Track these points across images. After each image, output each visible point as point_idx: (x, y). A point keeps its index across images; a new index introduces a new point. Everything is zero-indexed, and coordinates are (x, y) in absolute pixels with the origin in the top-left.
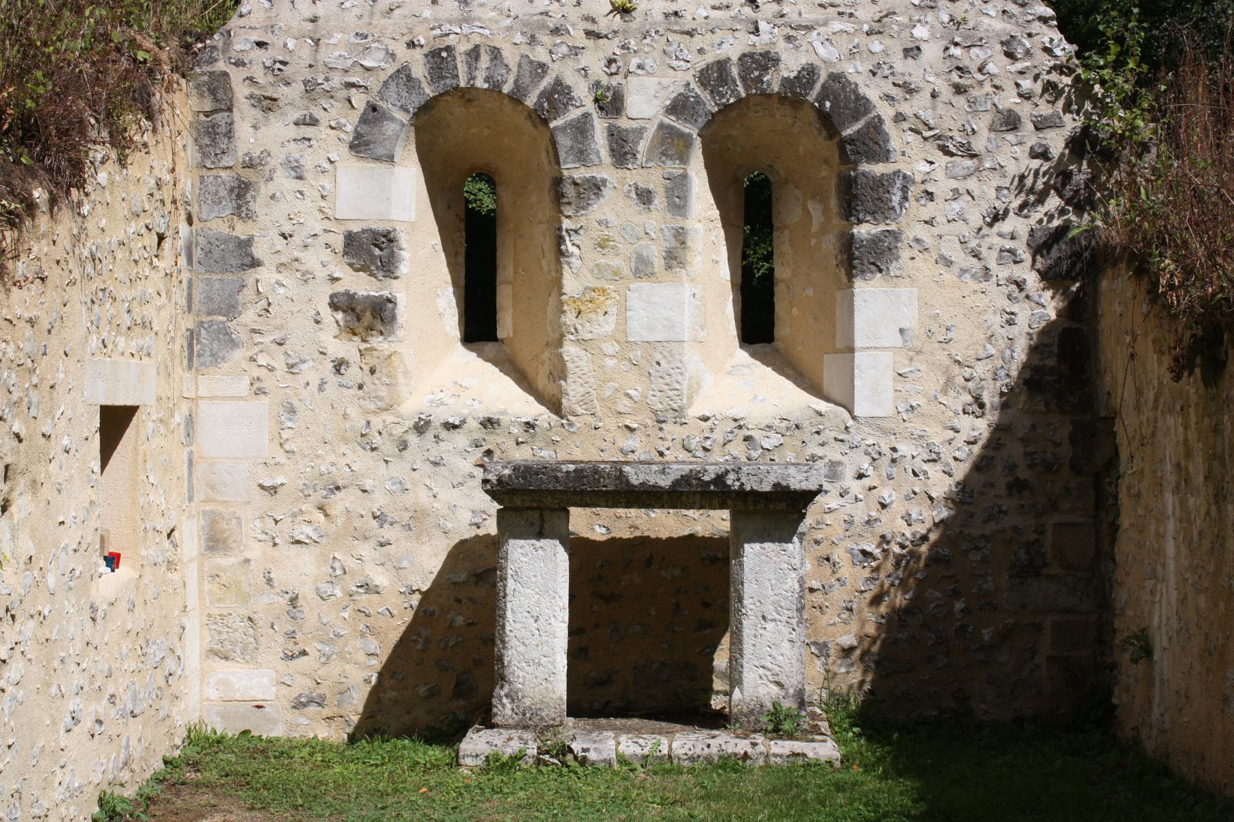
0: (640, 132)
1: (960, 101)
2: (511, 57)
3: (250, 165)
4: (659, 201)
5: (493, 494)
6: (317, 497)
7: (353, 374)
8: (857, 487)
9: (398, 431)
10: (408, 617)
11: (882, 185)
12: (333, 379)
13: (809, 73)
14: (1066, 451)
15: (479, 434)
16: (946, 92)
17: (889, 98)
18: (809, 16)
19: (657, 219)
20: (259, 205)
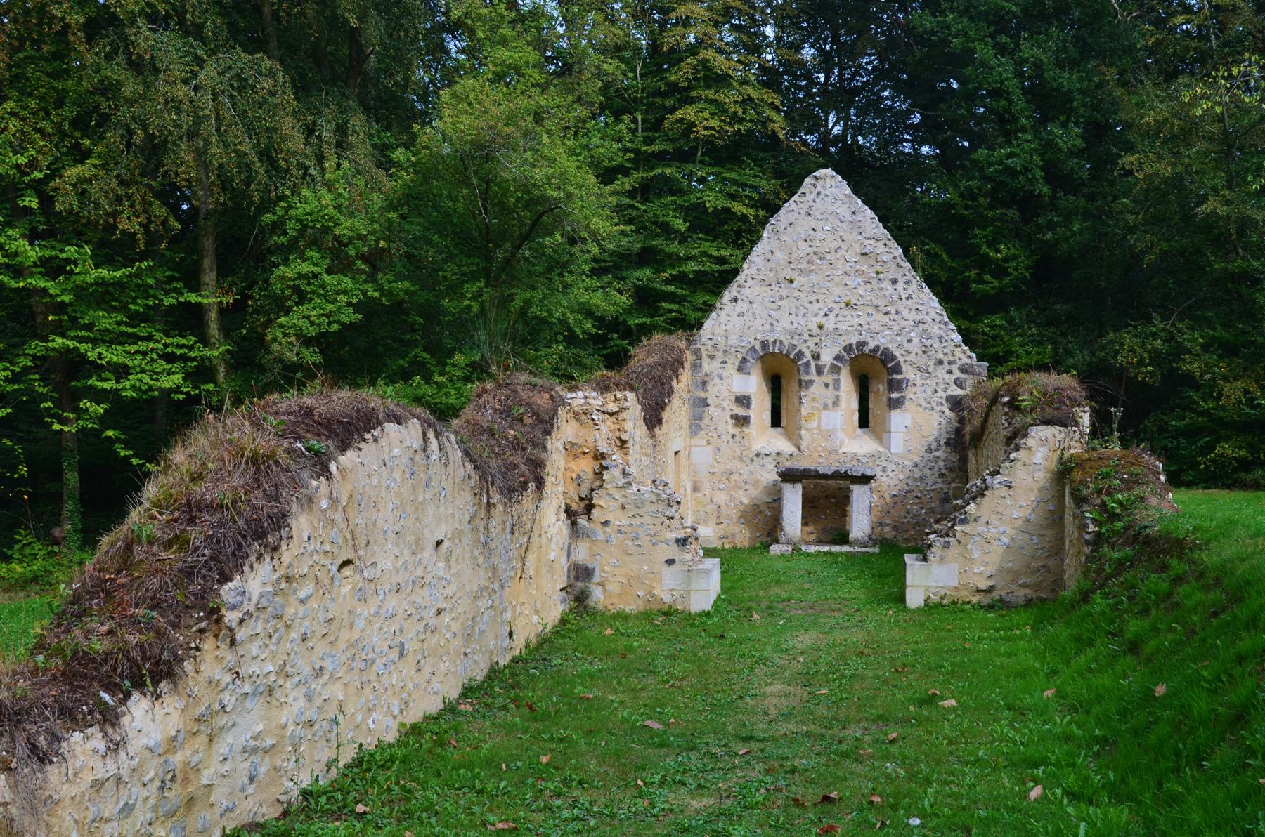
0: (825, 365)
1: (925, 356)
2: (786, 343)
4: (831, 387)
5: (780, 476)
7: (737, 439)
8: (892, 475)
11: (900, 381)
13: (877, 348)
16: (920, 353)
19: (830, 392)
20: (709, 388)
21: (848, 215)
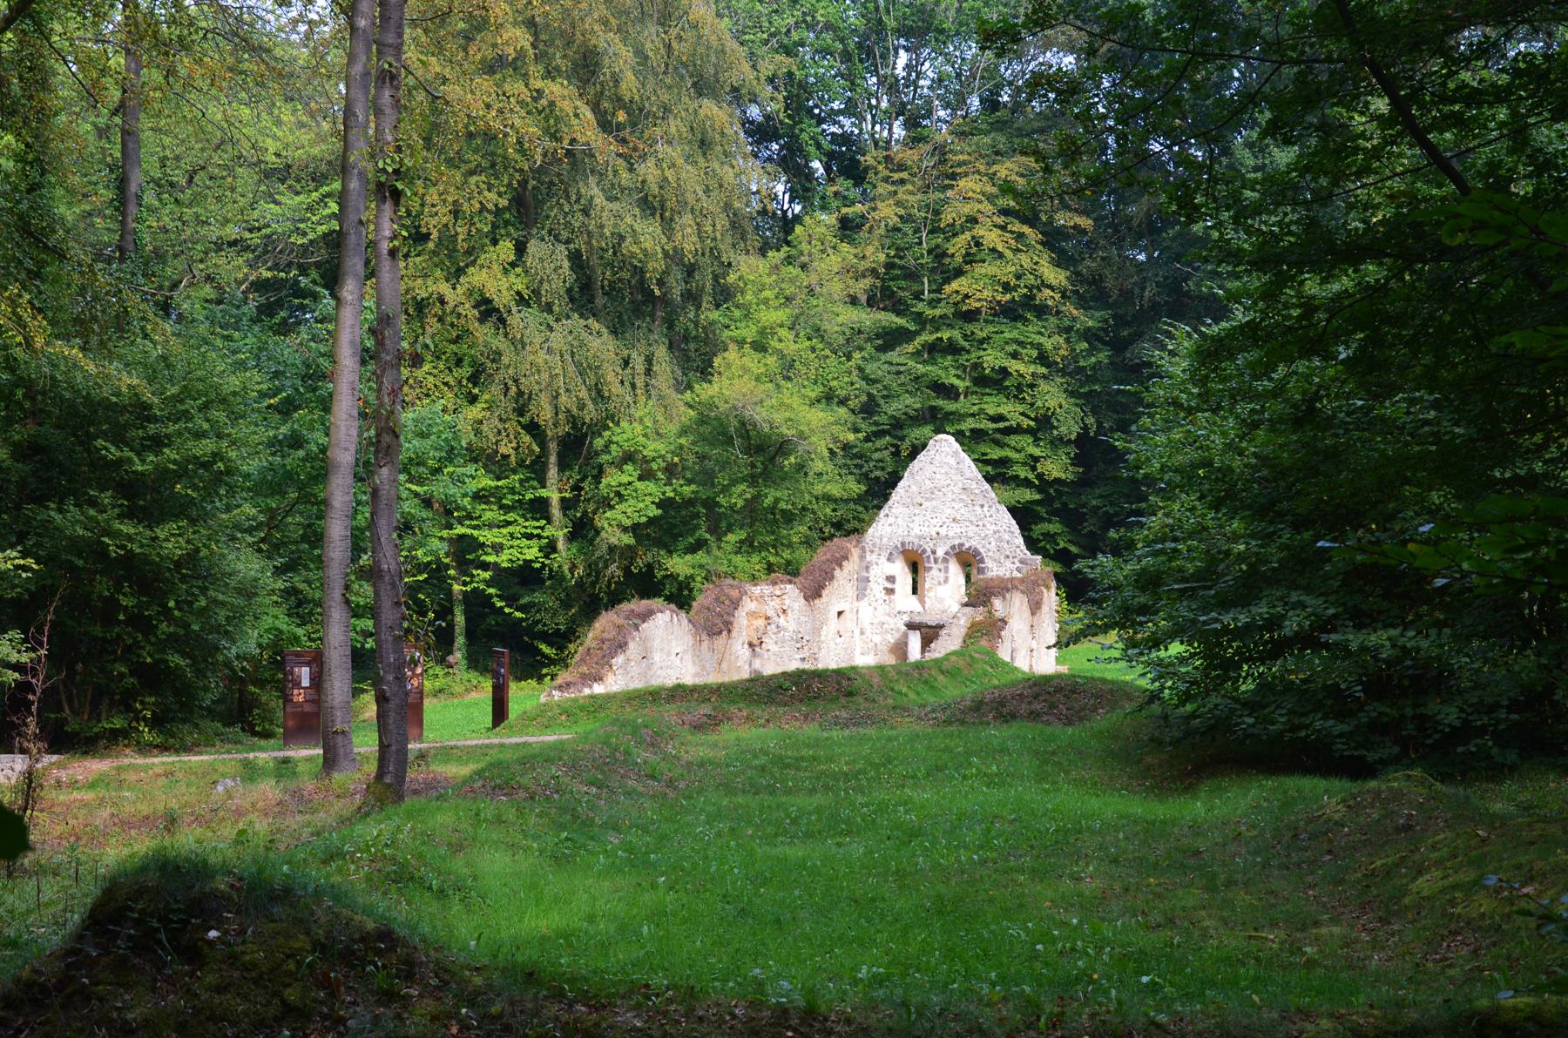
19: (942, 575)
21: (954, 464)
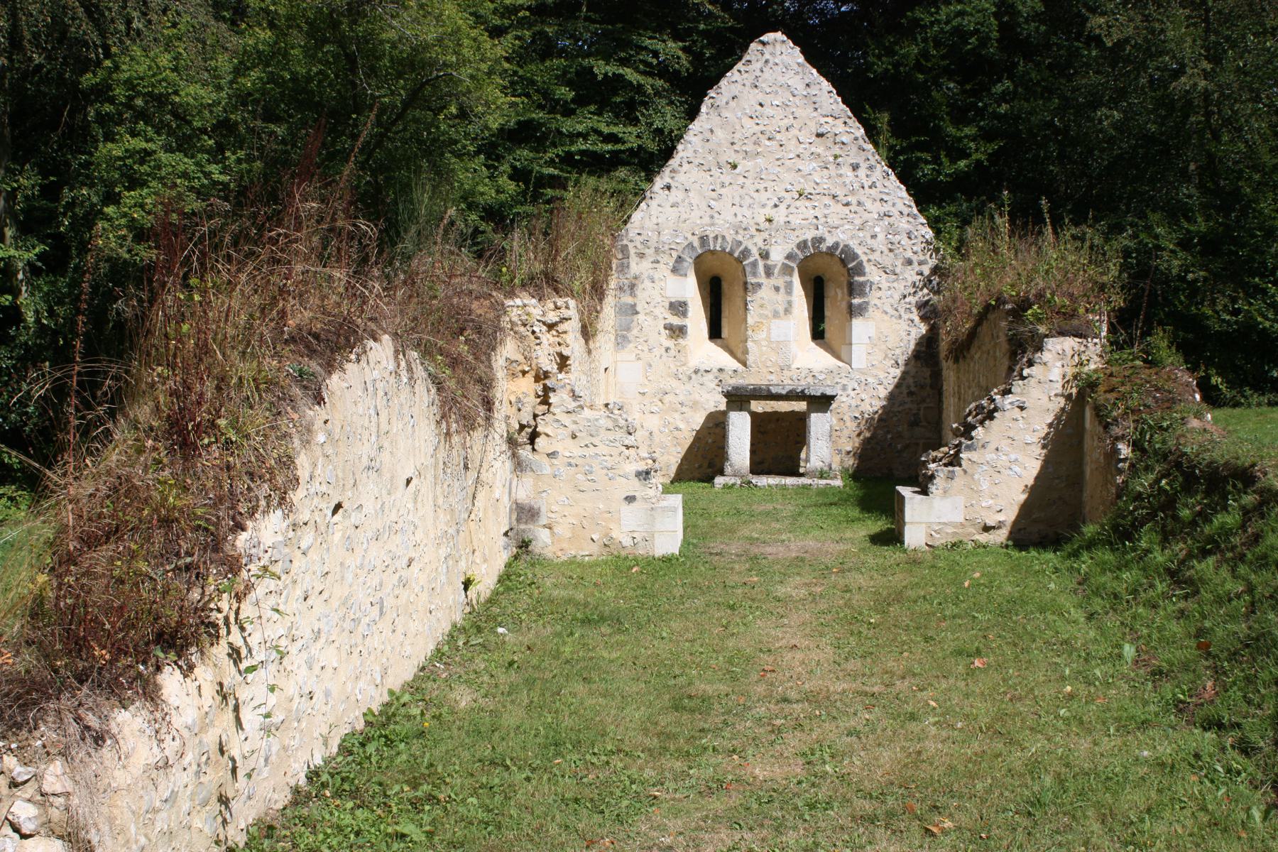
0: (776, 265)
1: (891, 255)
2: (729, 239)
3: (636, 278)
4: (782, 290)
5: (725, 396)
6: (659, 396)
7: (672, 352)
8: (853, 394)
9: (688, 373)
10: (691, 440)
11: (862, 285)
12: (664, 354)
13: (837, 245)
14: (928, 381)
15: (717, 374)
16: (886, 251)
17: (866, 253)
18: (837, 222)
19: (781, 297)
20: (638, 292)
21: (801, 89)
